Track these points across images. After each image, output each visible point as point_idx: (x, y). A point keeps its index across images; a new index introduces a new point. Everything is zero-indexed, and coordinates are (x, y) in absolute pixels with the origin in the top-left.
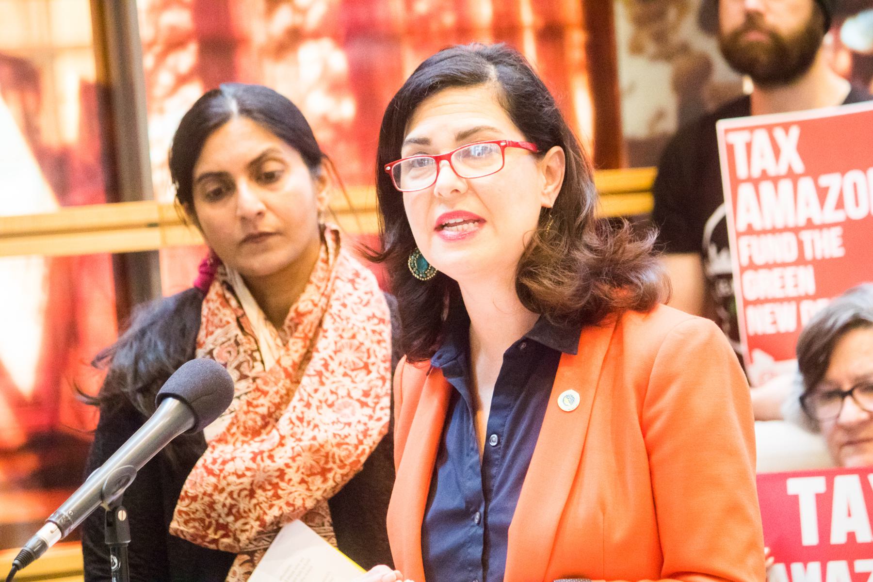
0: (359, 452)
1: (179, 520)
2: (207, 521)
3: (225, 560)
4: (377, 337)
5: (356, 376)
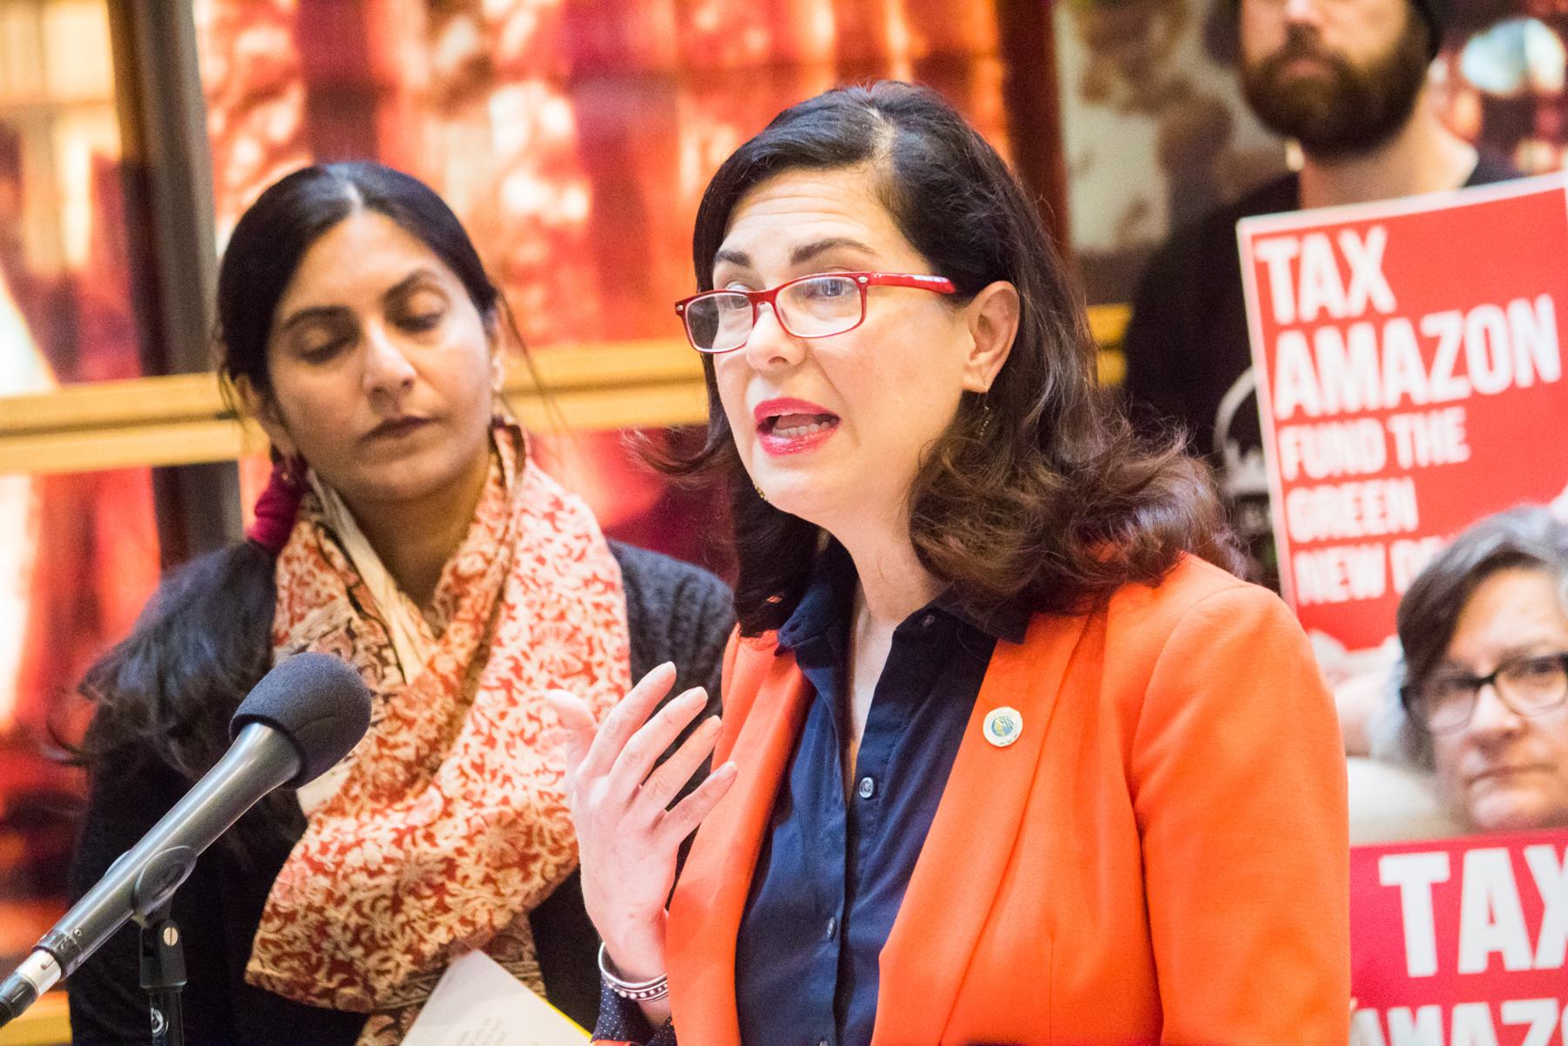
3: (353, 1022)
4: (603, 616)
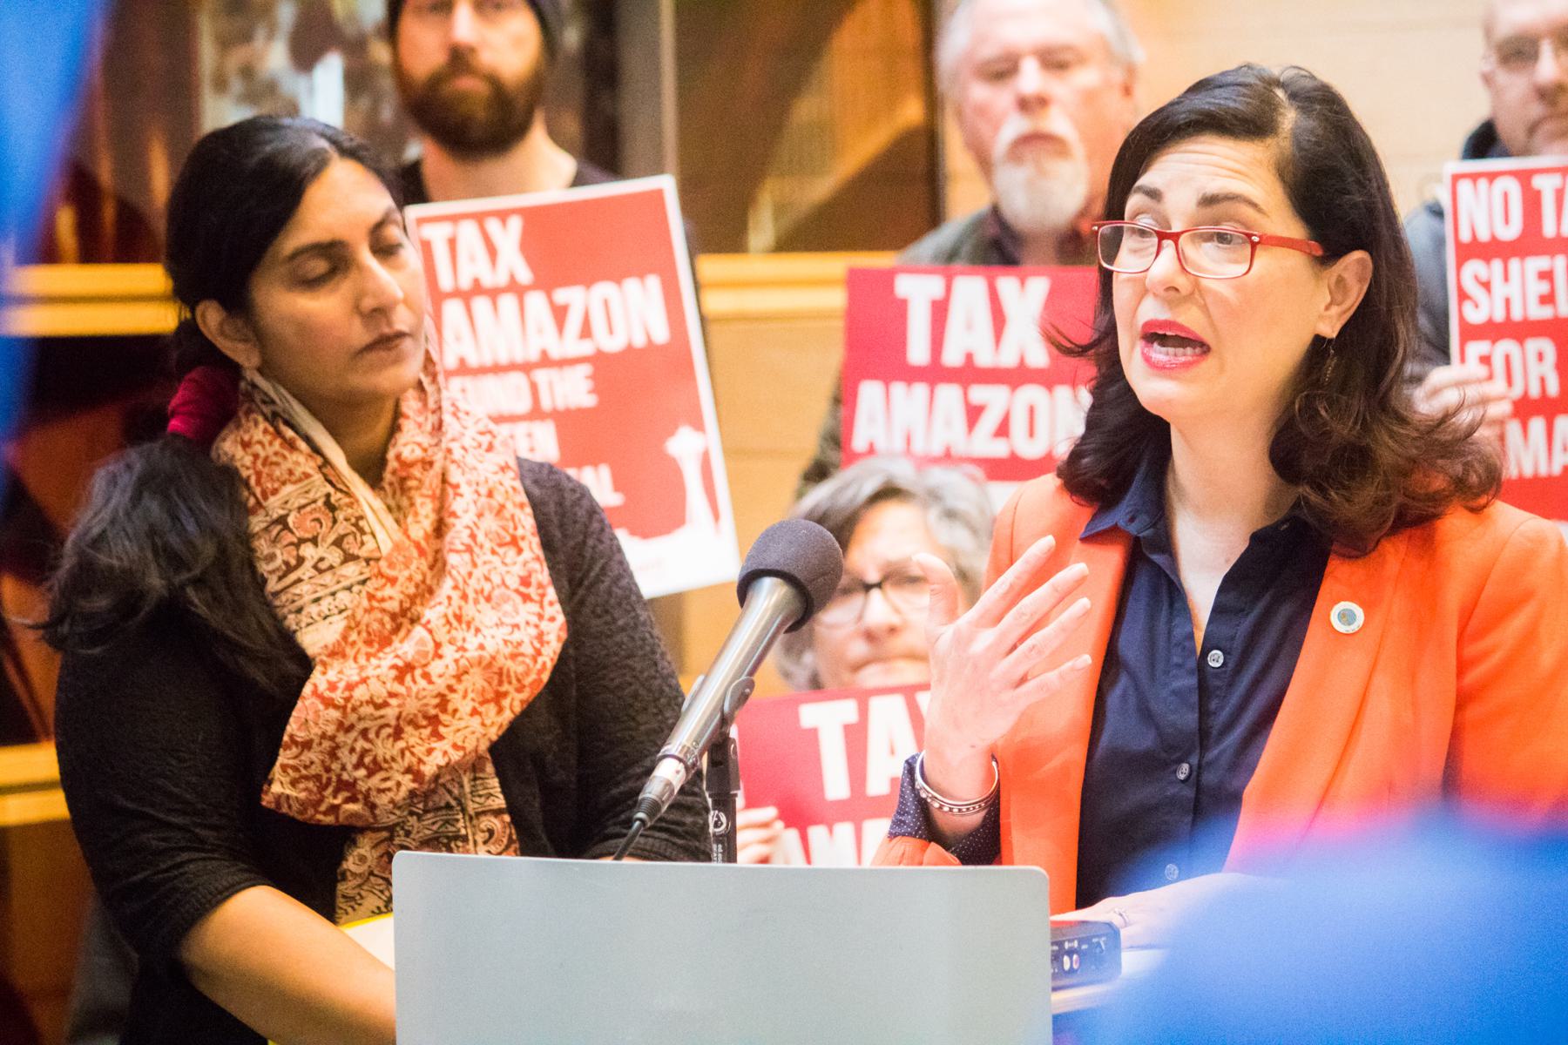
0: (539, 666)
1: (283, 779)
2: (325, 777)
5: (505, 554)
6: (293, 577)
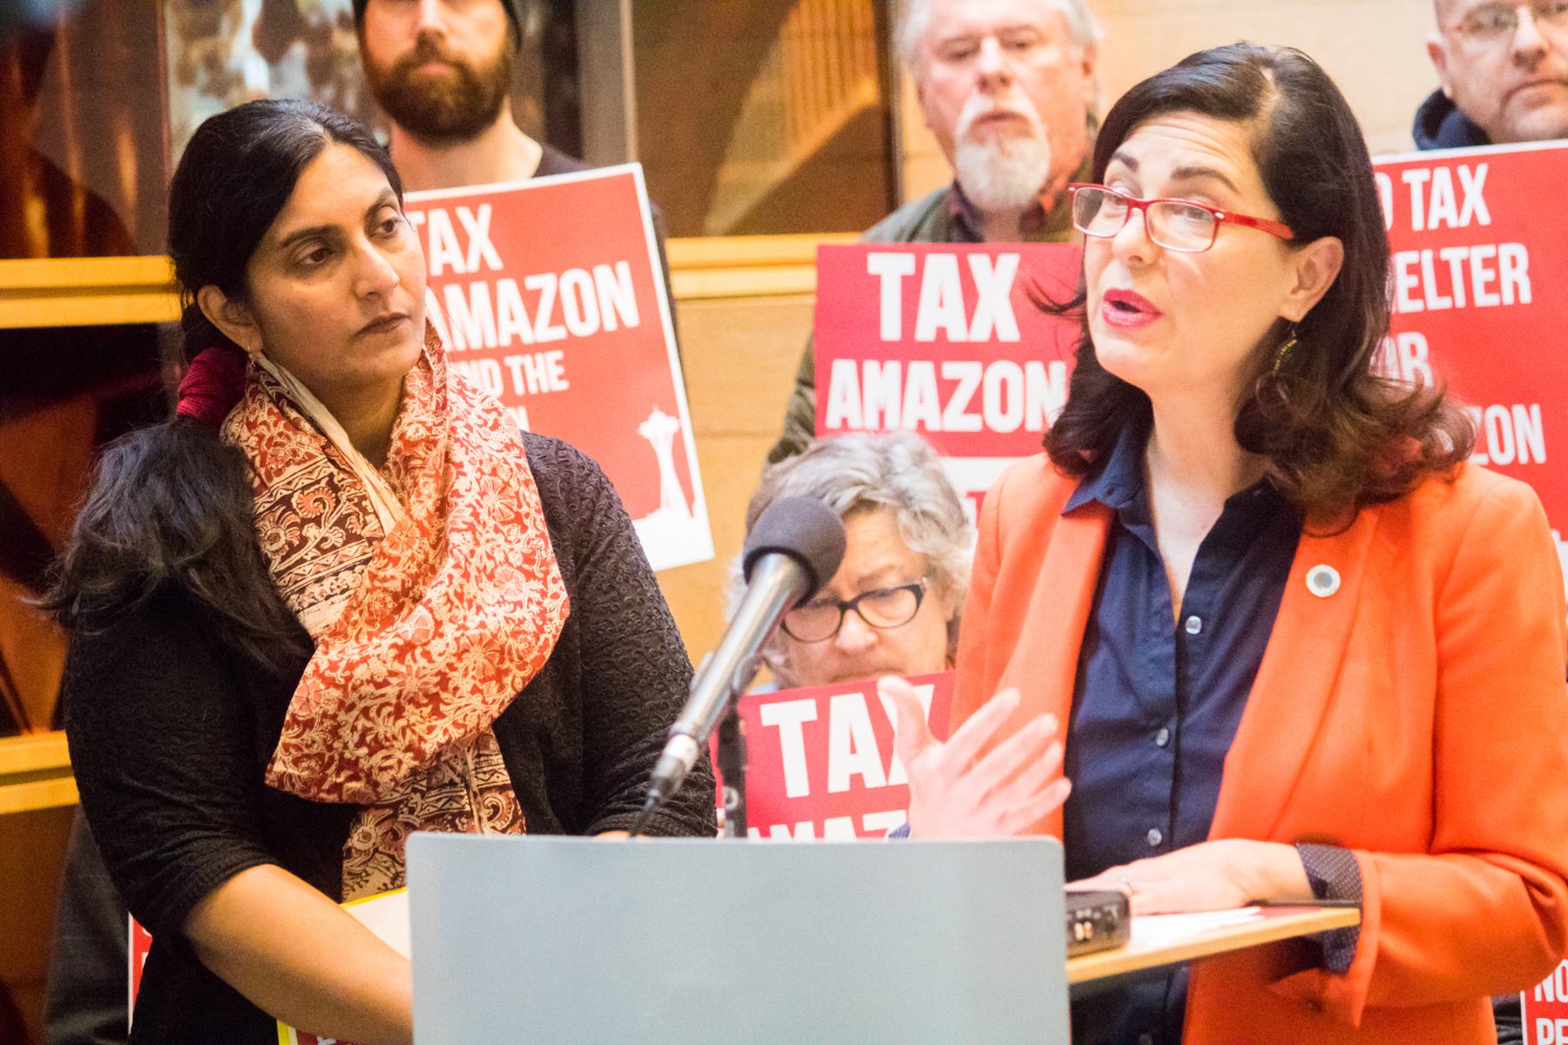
0: (541, 643)
1: (286, 758)
2: (328, 755)
4: (523, 477)
5: (509, 531)
6: (295, 557)
